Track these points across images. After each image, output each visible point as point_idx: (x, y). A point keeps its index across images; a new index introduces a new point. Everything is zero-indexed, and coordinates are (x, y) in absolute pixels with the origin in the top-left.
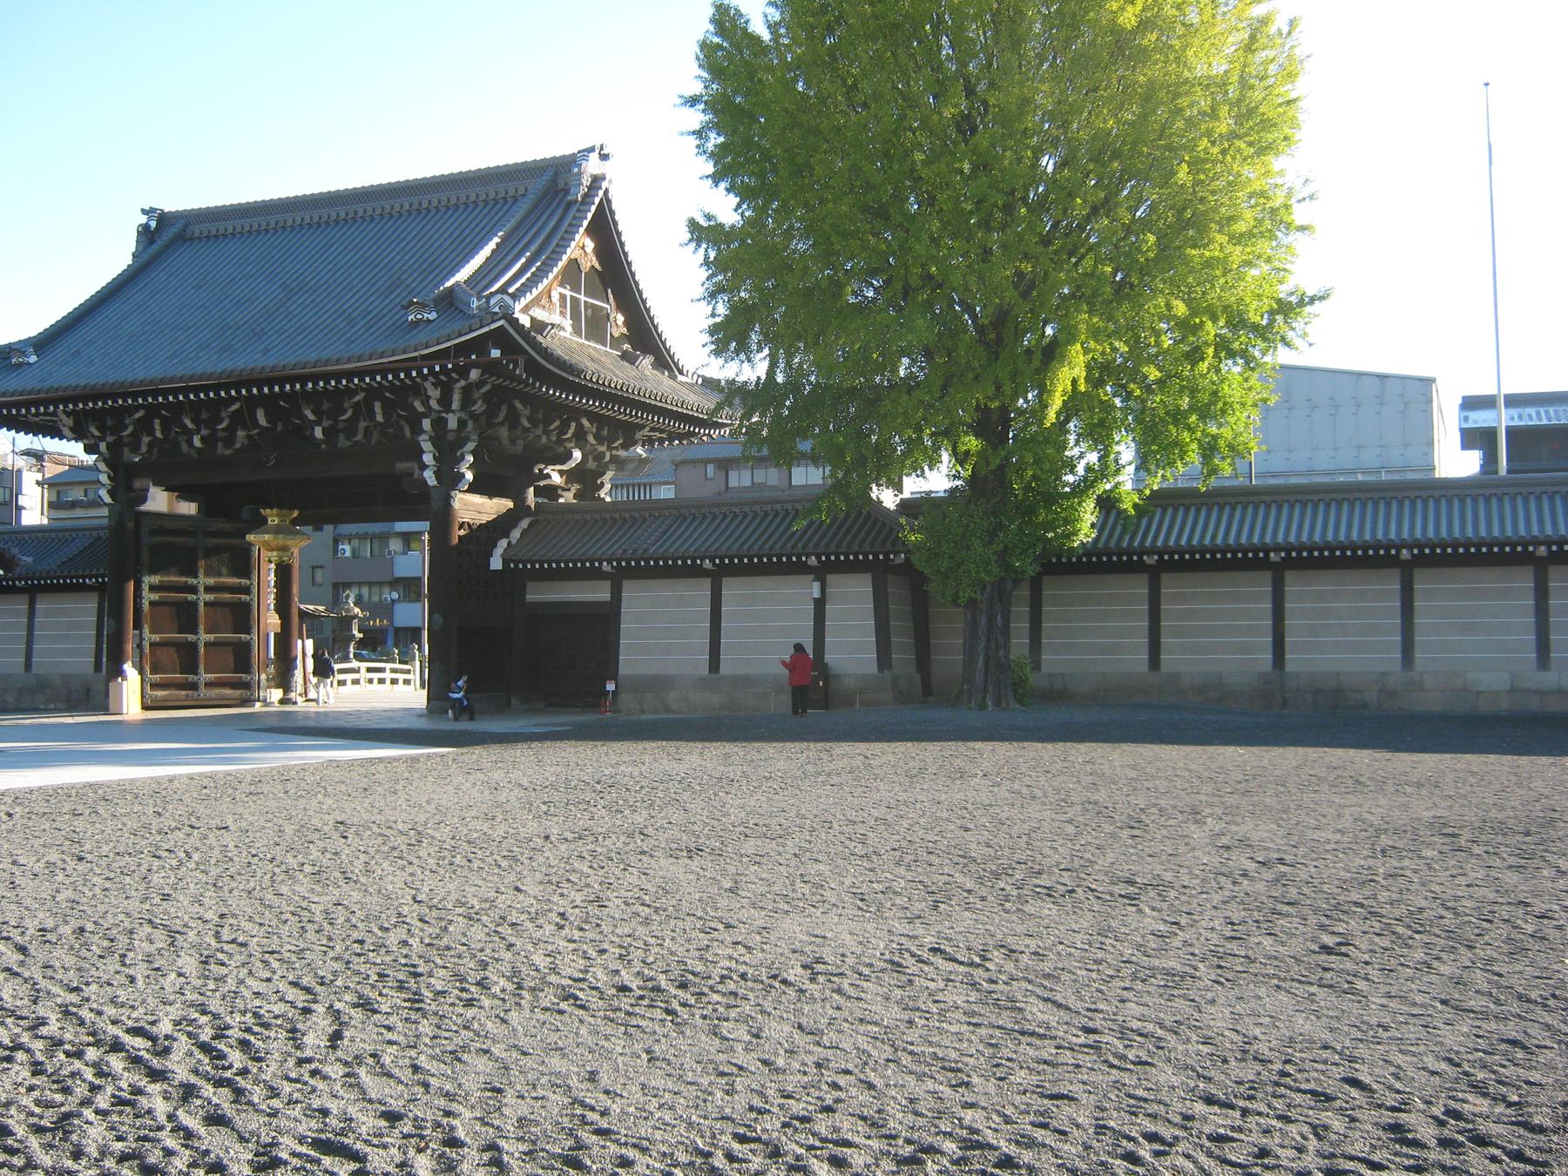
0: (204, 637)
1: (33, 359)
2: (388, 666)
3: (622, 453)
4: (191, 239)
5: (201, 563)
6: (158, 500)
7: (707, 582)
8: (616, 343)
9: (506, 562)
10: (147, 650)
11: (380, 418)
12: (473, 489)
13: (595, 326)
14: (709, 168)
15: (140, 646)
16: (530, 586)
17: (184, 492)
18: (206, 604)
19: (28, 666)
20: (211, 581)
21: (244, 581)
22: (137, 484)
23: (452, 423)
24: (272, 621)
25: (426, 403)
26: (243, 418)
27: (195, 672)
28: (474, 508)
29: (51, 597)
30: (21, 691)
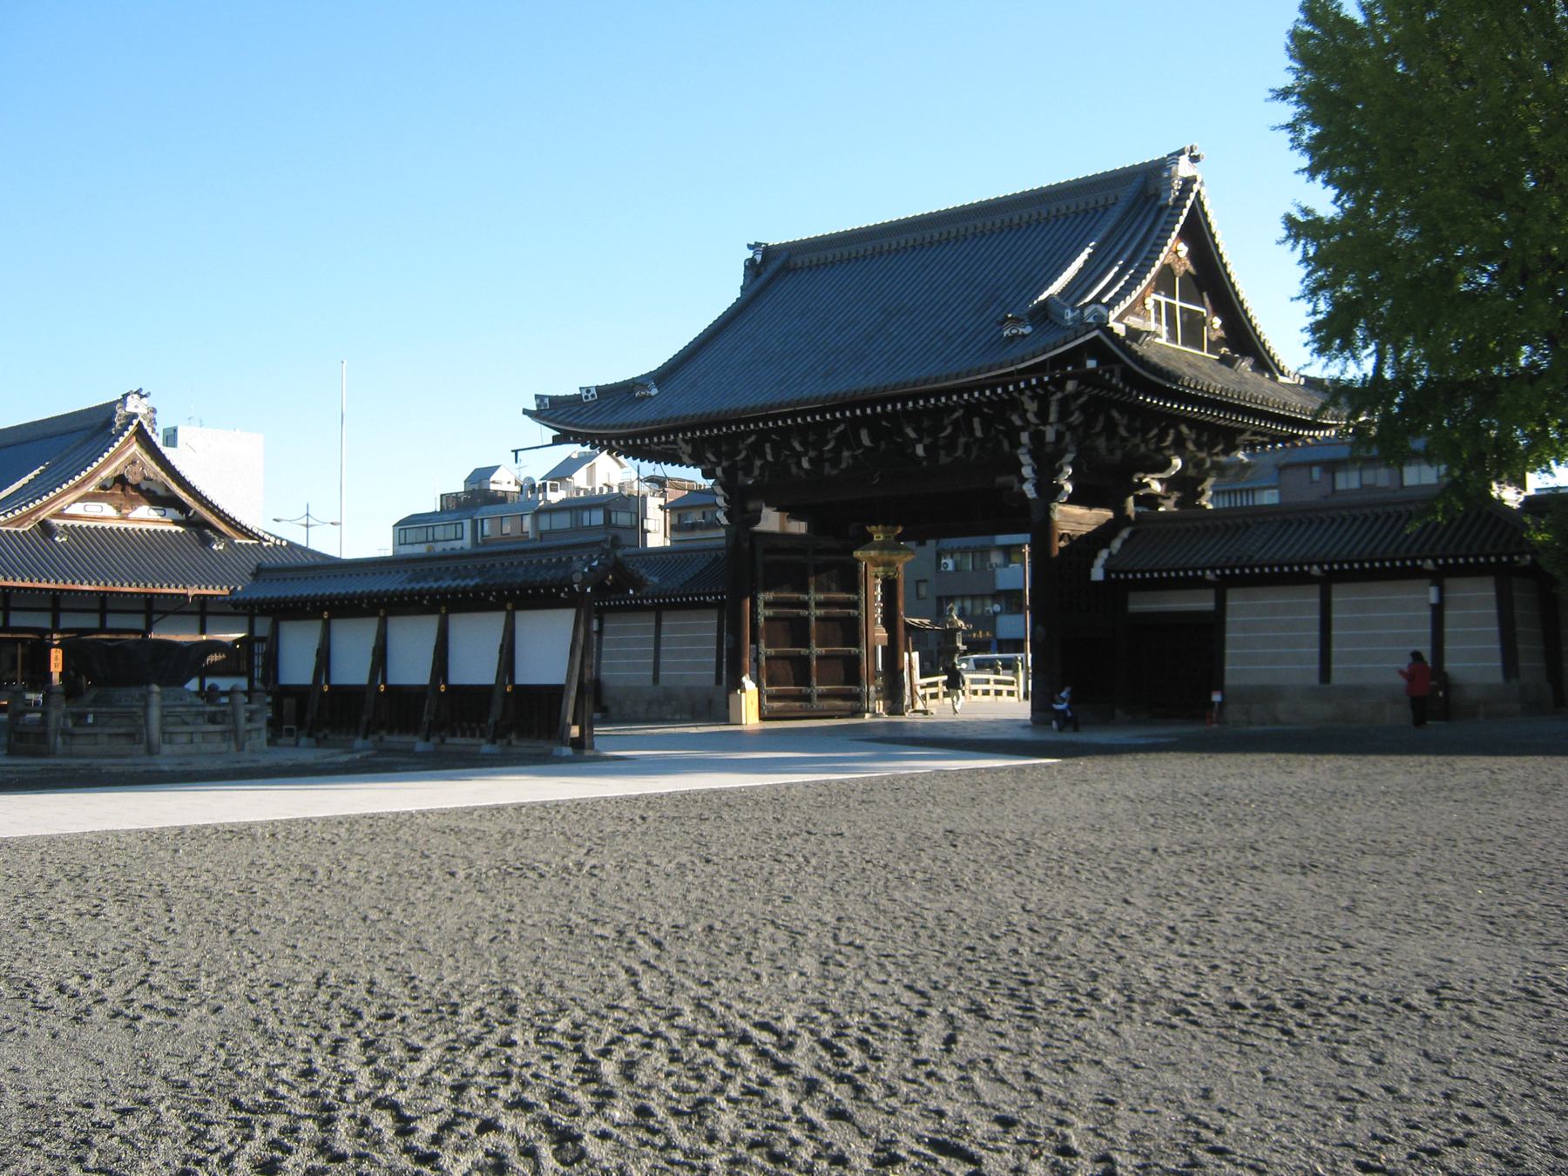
1: (654, 392)
3: (1223, 459)
4: (795, 270)
5: (812, 580)
6: (771, 521)
7: (1316, 589)
8: (1213, 347)
9: (1107, 572)
11: (979, 433)
12: (1073, 500)
13: (1192, 331)
14: (1305, 162)
15: (757, 660)
16: (1132, 596)
17: (794, 513)
18: (818, 619)
19: (656, 679)
20: (821, 597)
21: (852, 596)
22: (751, 506)
23: (1050, 435)
24: (880, 634)
25: (1023, 417)
26: (848, 439)
27: (808, 683)
28: (1074, 519)
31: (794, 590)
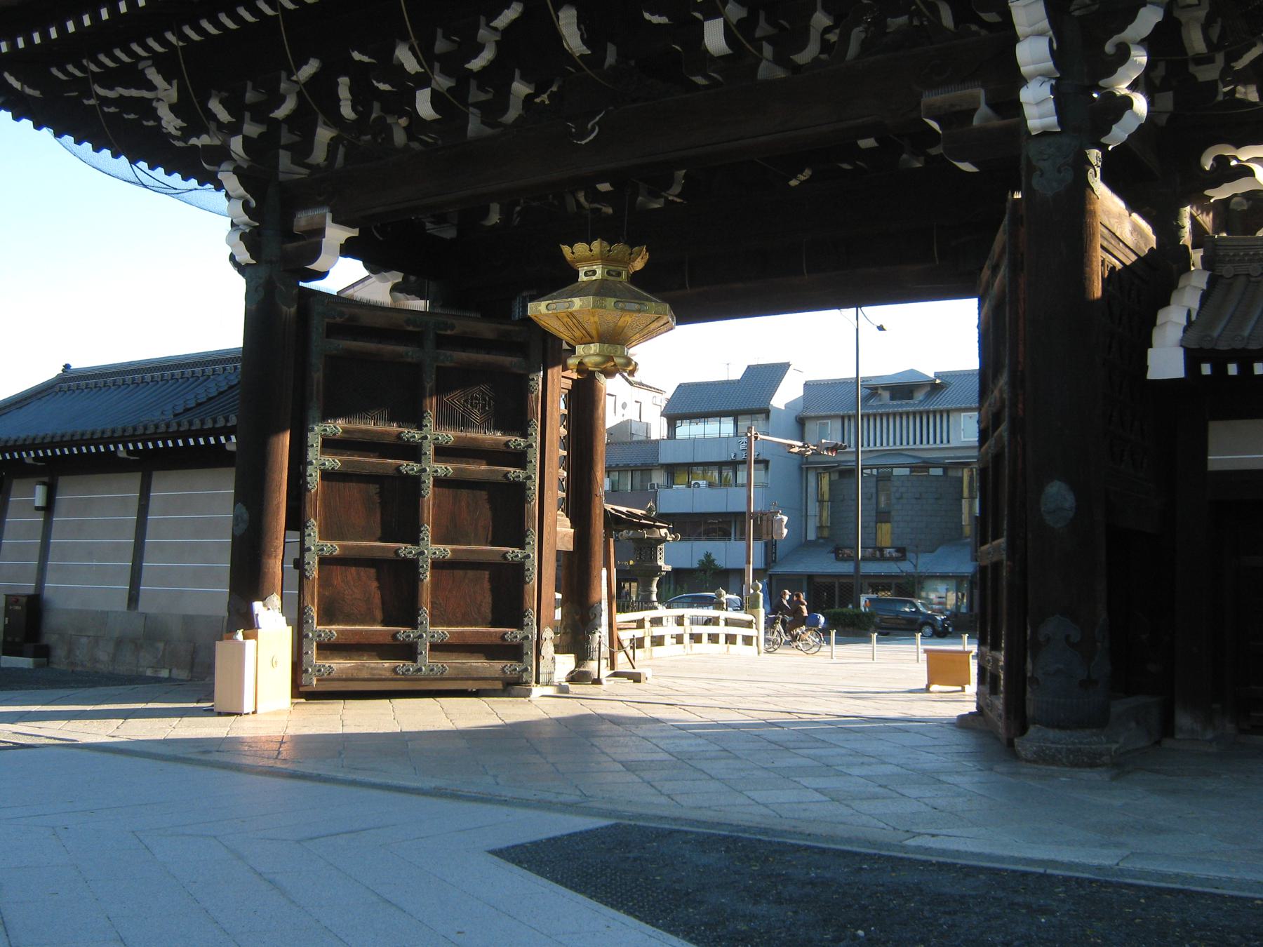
0: (432, 549)
2: (723, 615)
9: (1193, 358)
10: (313, 571)
15: (299, 564)
16: (1218, 432)
18: (439, 482)
19: (133, 599)
20: (449, 436)
21: (516, 441)
22: (303, 220)
24: (561, 531)
29: (174, 477)
30: (119, 643)
31: (396, 416)
